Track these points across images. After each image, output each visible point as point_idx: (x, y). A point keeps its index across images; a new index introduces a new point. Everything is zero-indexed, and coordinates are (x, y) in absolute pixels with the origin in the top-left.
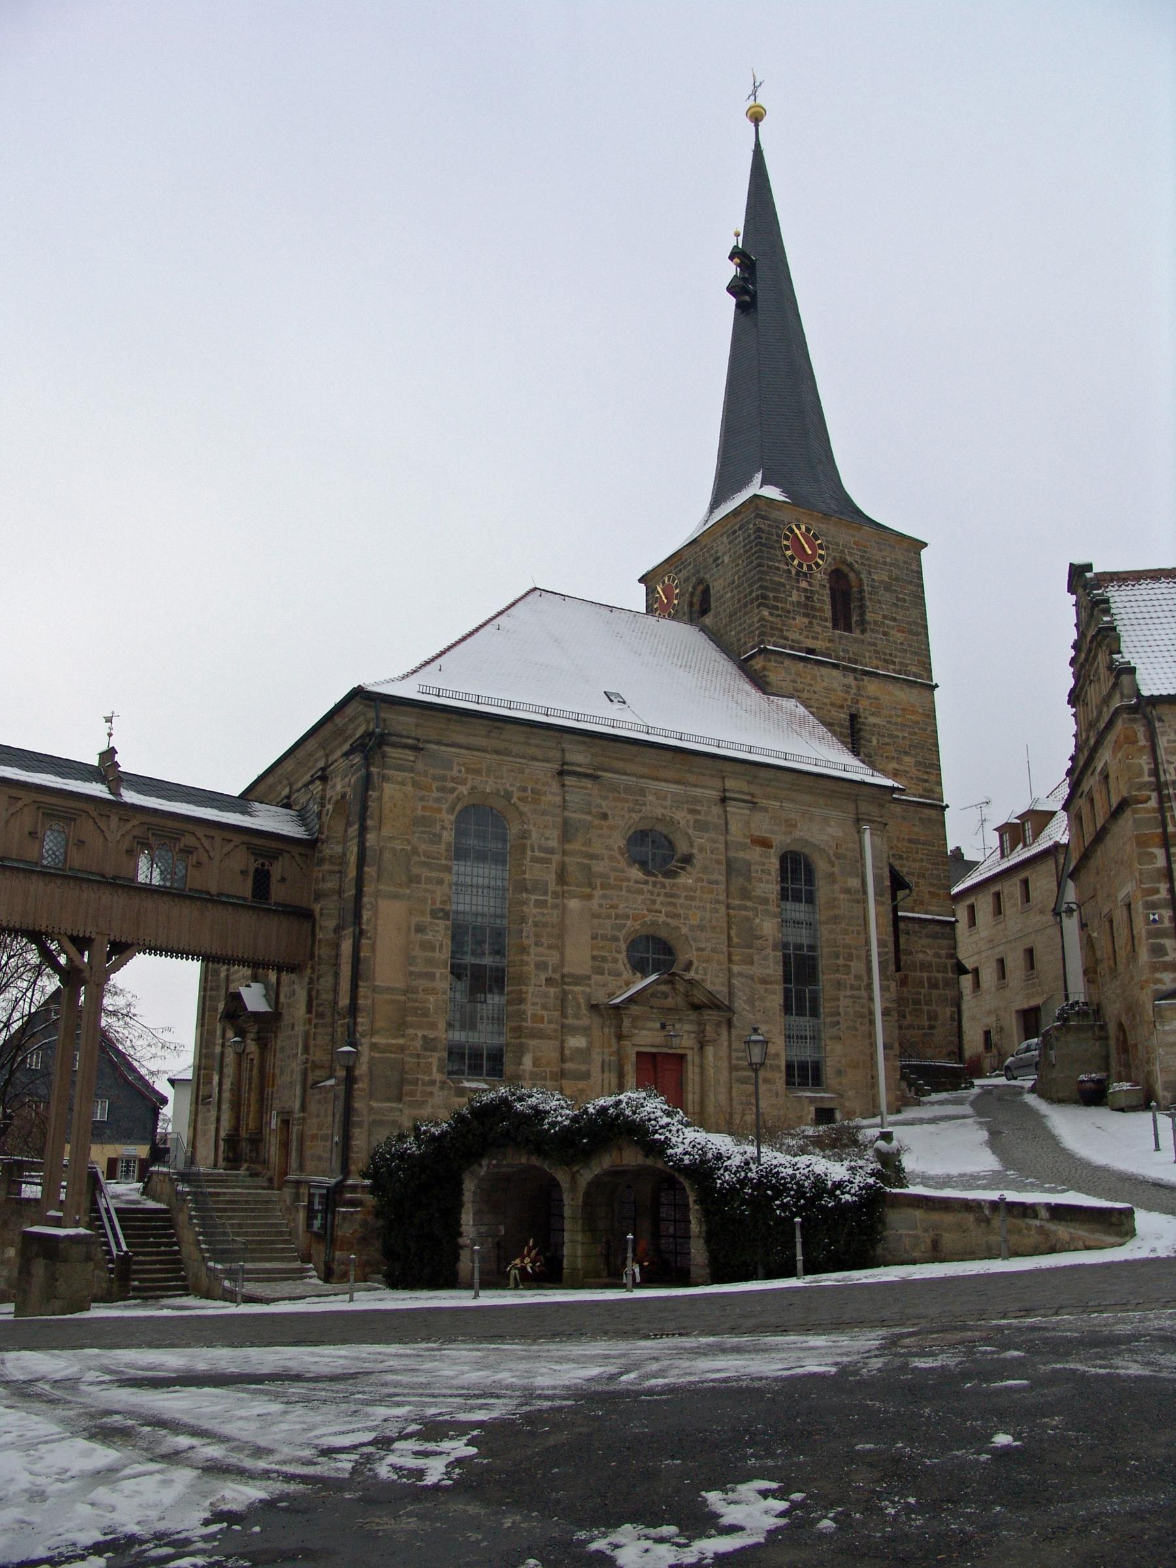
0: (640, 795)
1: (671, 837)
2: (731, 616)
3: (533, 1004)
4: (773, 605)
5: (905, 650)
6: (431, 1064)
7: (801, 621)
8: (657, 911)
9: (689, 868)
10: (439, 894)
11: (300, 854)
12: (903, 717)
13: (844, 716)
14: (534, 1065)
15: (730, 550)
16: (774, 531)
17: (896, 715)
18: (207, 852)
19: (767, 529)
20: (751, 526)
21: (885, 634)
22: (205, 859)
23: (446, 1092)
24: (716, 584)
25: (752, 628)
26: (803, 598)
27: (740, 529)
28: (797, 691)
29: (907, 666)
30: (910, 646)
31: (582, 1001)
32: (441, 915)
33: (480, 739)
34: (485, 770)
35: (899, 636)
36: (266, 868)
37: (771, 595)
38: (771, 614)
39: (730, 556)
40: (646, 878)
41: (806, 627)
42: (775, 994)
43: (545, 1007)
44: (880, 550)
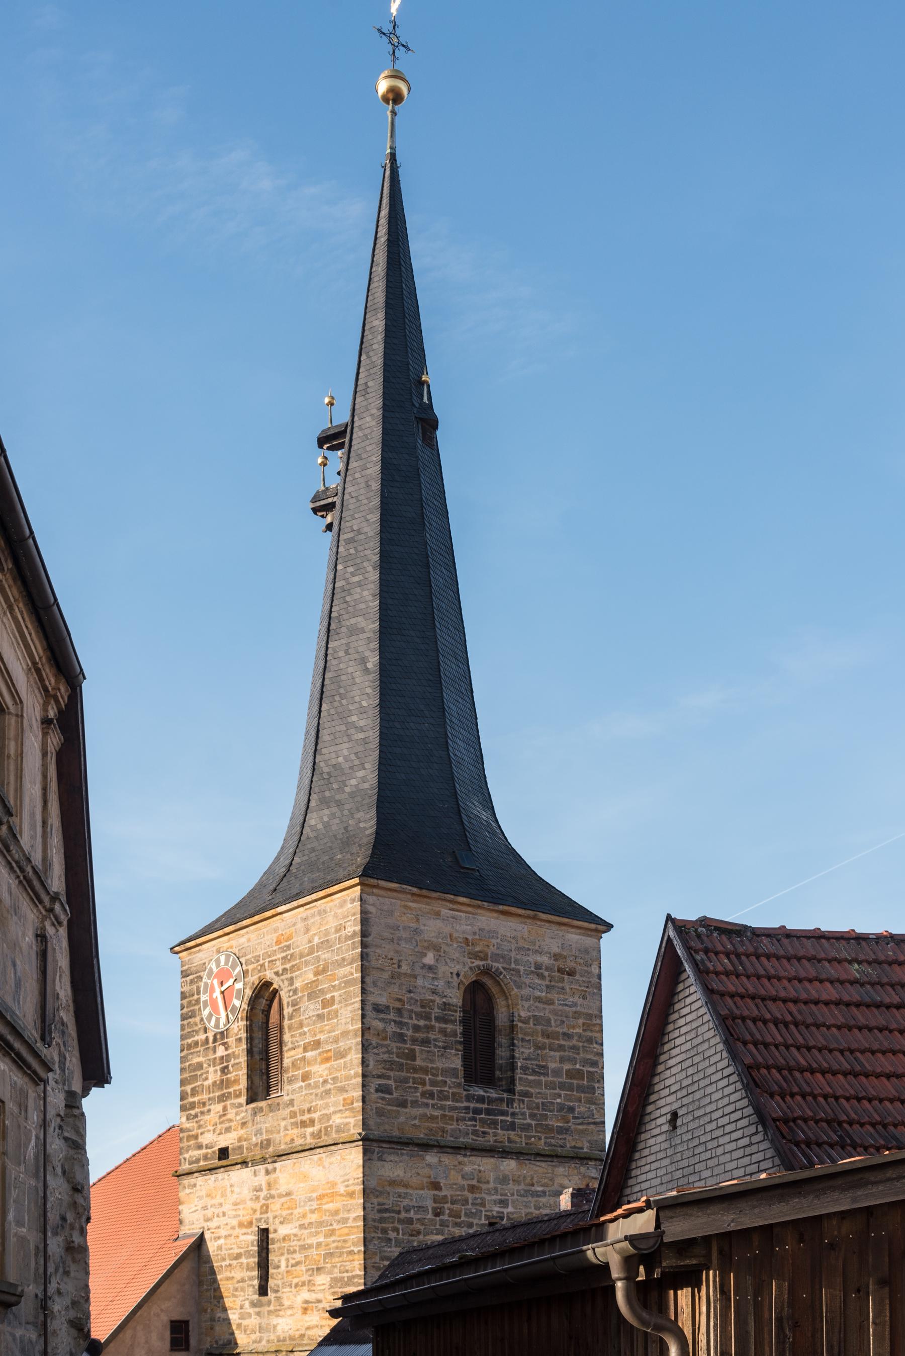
13: (251, 1238)
17: (312, 1211)
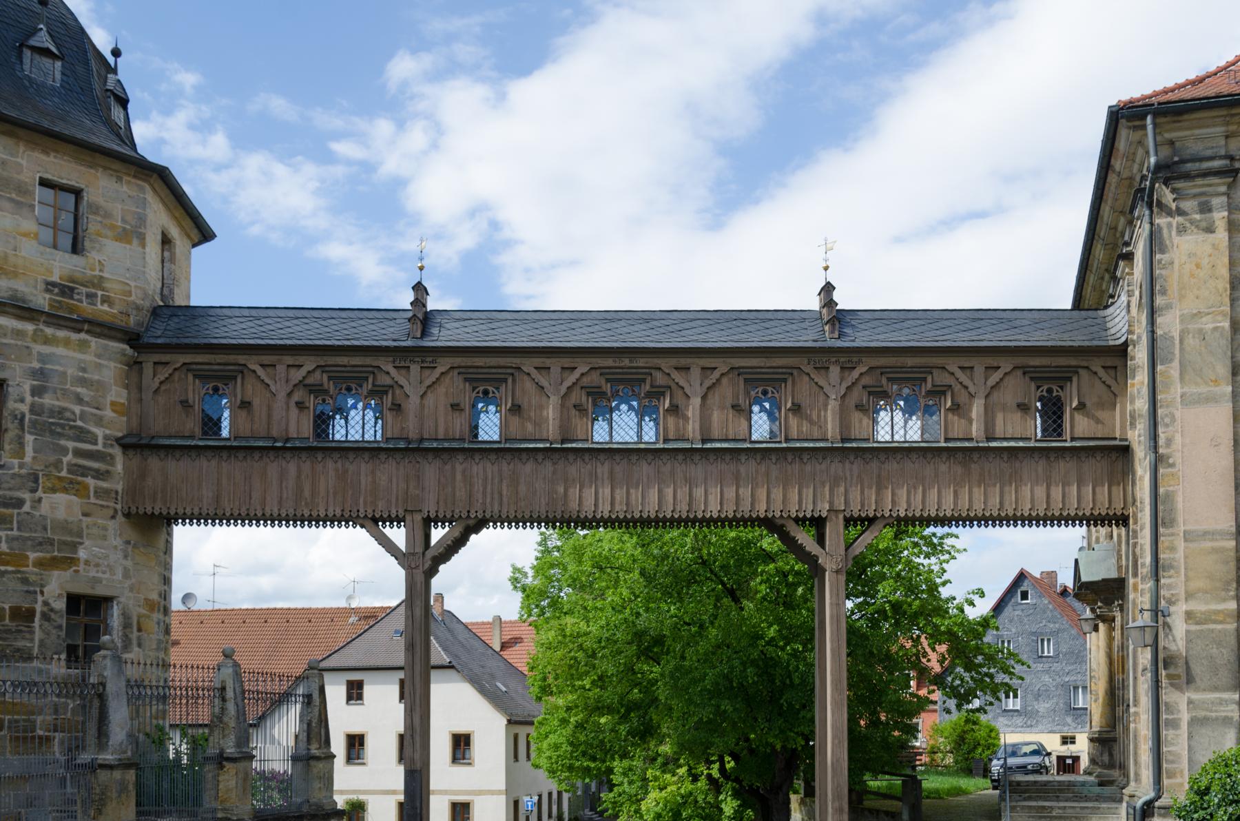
11: (1103, 367)
18: (966, 387)
22: (962, 398)
36: (1054, 394)
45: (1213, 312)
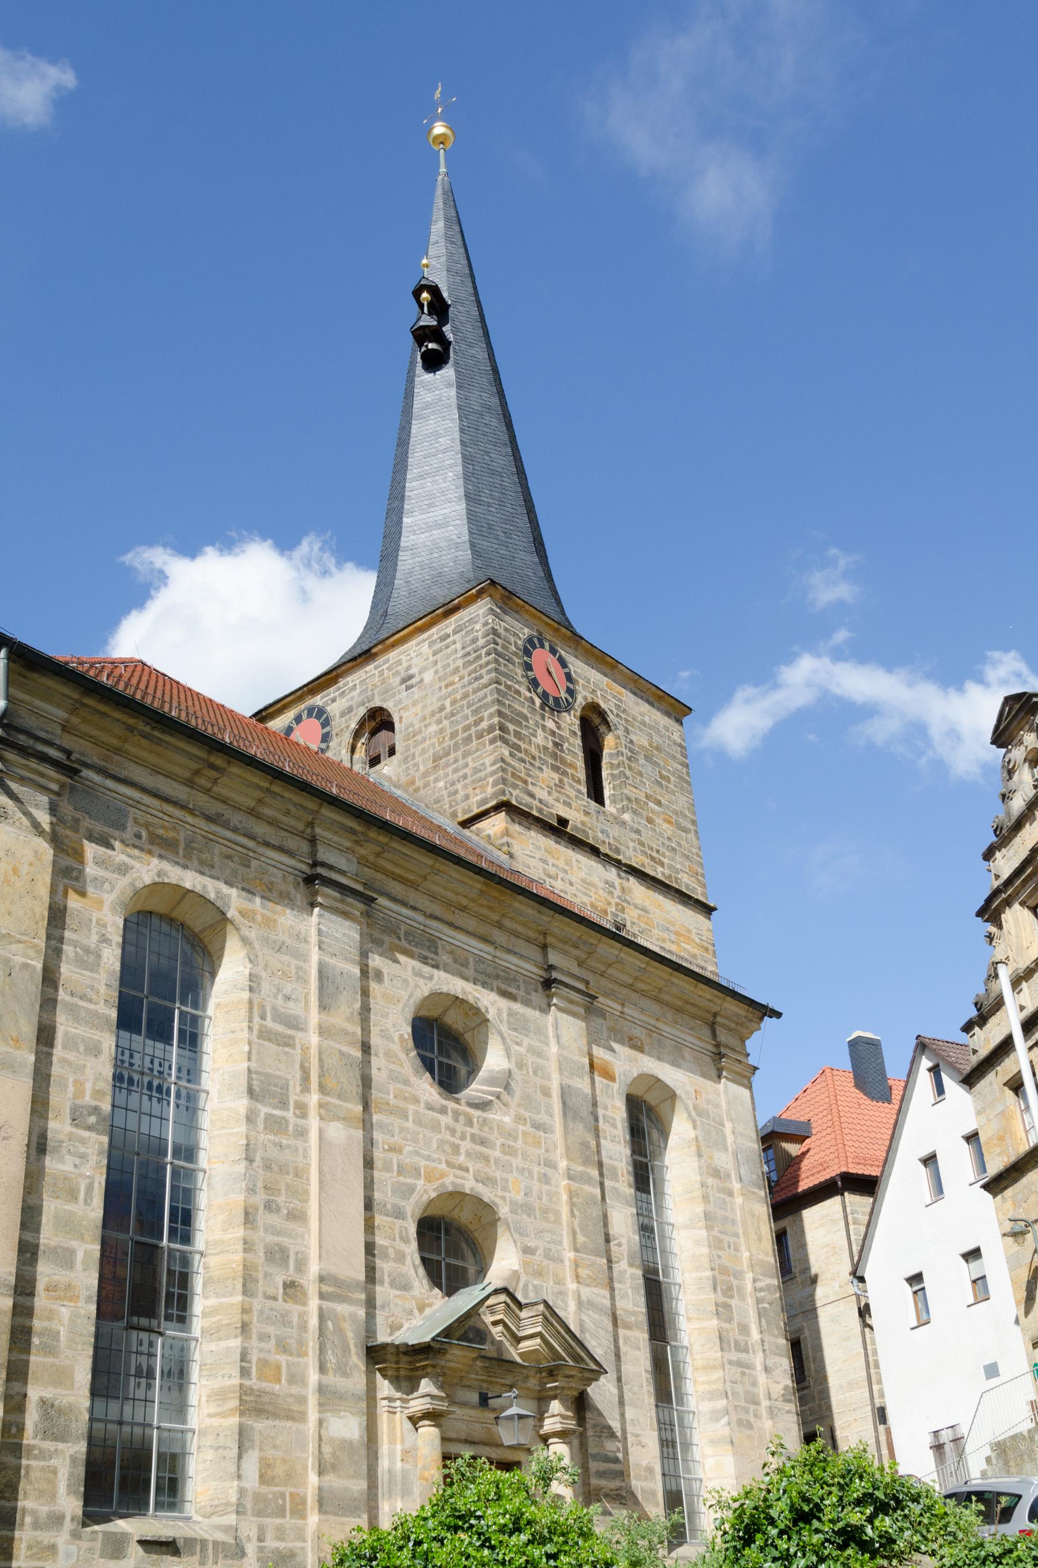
0: (429, 949)
1: (468, 1037)
2: (436, 758)
3: (263, 1337)
4: (514, 744)
5: (674, 850)
6: (55, 1472)
7: (549, 775)
8: (461, 1168)
9: (505, 1096)
10: (89, 1073)
12: (679, 945)
14: (263, 1479)
15: (436, 663)
16: (512, 639)
17: (670, 940)
19: (501, 631)
20: (478, 627)
21: (650, 821)
23: (85, 1545)
24: (405, 714)
25: (482, 774)
26: (550, 745)
27: (455, 632)
28: (550, 877)
29: (677, 872)
30: (679, 845)
31: (350, 1335)
32: (92, 1119)
33: (175, 784)
34: (182, 845)
35: (667, 829)
37: (511, 727)
38: (512, 755)
39: (436, 672)
40: (445, 1102)
41: (556, 785)
42: (639, 1349)
43: (283, 1347)
44: (637, 704)
45: (25, 942)
